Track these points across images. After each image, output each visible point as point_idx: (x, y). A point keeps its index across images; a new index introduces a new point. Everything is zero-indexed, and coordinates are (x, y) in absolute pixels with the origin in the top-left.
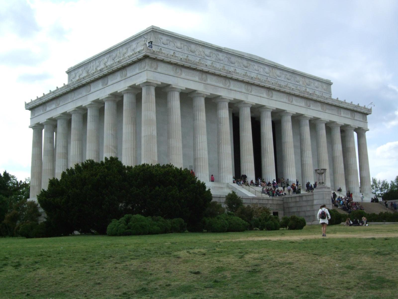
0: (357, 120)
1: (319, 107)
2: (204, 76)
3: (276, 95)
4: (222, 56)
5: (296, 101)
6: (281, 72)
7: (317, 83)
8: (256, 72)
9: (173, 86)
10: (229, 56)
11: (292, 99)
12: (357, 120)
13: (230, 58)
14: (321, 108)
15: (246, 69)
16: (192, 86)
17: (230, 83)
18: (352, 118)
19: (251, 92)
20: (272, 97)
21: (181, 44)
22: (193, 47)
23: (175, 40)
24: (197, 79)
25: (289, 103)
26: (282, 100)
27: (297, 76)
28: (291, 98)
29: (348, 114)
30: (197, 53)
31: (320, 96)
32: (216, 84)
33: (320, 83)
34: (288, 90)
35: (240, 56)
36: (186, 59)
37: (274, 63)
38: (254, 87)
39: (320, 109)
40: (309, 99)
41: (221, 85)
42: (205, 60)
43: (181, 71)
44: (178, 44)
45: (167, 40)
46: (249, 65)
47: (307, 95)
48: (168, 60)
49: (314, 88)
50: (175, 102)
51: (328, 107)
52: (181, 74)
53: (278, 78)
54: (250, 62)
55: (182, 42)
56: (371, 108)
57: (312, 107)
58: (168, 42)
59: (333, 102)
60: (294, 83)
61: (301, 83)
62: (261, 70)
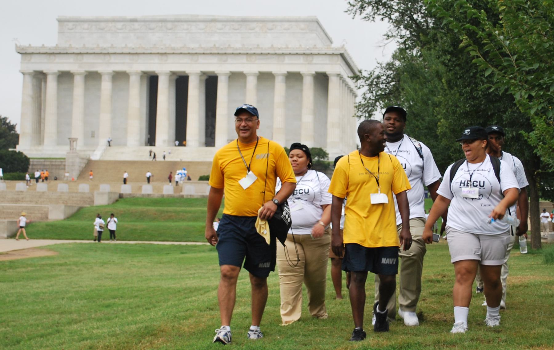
0: (315, 64)
1: (244, 59)
2: (79, 57)
6: (224, 23)
7: (286, 25)
8: (186, 31)
12: (315, 64)
15: (170, 31)
16: (65, 68)
22: (103, 25)
29: (301, 59)
33: (293, 23)
40: (223, 54)
44: (86, 25)
48: (38, 51)
50: (51, 85)
53: (218, 31)
54: (176, 23)
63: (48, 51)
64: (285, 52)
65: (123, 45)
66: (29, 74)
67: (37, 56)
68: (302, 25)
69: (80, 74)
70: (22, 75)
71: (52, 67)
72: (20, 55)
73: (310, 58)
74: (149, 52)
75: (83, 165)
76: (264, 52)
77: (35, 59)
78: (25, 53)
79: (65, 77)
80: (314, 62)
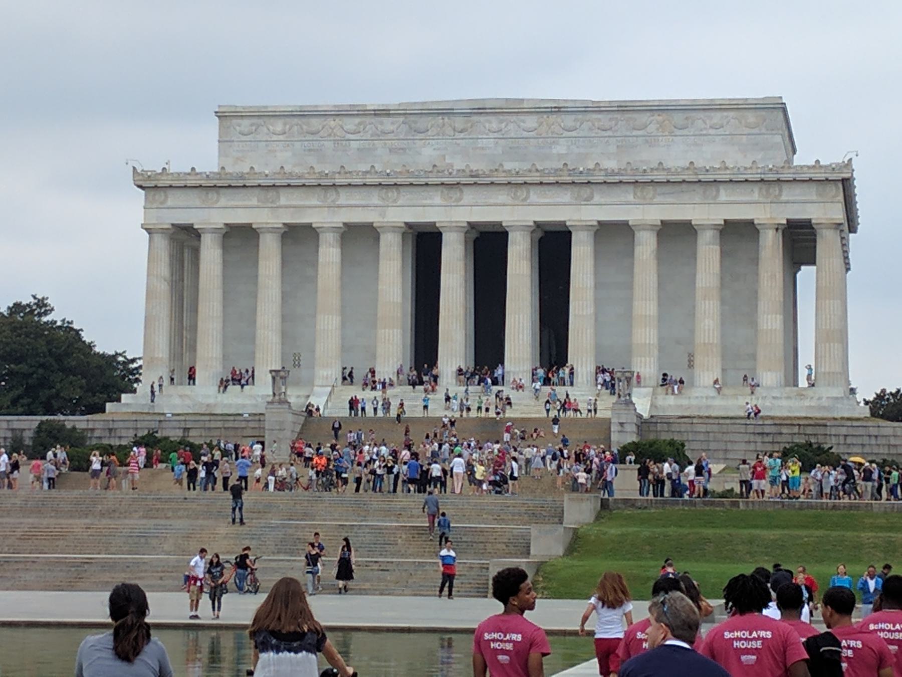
2: (271, 194)
3: (469, 196)
4: (393, 123)
5: (534, 195)
6: (580, 116)
7: (717, 117)
8: (496, 135)
9: (196, 227)
10: (412, 118)
11: (528, 193)
13: (415, 122)
14: (635, 194)
15: (462, 135)
16: (240, 217)
17: (338, 193)
18: (769, 200)
19: (395, 201)
20: (461, 199)
21: (285, 124)
22: (316, 123)
23: (272, 120)
24: (254, 202)
25: (516, 202)
26: (492, 201)
27: (635, 115)
28: (522, 193)
29: (756, 194)
30: (321, 134)
31: (616, 171)
32: (302, 203)
34: (504, 180)
35: (446, 112)
36: (219, 174)
37: (554, 101)
38: (402, 189)
39: (631, 198)
40: (583, 184)
41: (314, 202)
42: (344, 143)
43: (218, 194)
44: (279, 126)
45: (252, 125)
46: (469, 125)
47: (568, 178)
49: (704, 132)
51: (660, 189)
52: (217, 201)
54: (475, 118)
55: (288, 120)
56: (851, 159)
57: (597, 198)
58: (254, 128)
59: (669, 177)
60: (628, 133)
61: (652, 128)
62: (511, 126)
63: (204, 183)
64: (719, 178)
65: (366, 167)
66: (163, 231)
67: (178, 192)
68: (751, 117)
69: (273, 230)
70: (148, 235)
71: (212, 215)
72: (143, 192)
73: (774, 190)
74: (423, 181)
75: (298, 429)
76: (673, 178)
77: (174, 198)
78: (153, 186)
79: (239, 238)
80: (784, 198)
